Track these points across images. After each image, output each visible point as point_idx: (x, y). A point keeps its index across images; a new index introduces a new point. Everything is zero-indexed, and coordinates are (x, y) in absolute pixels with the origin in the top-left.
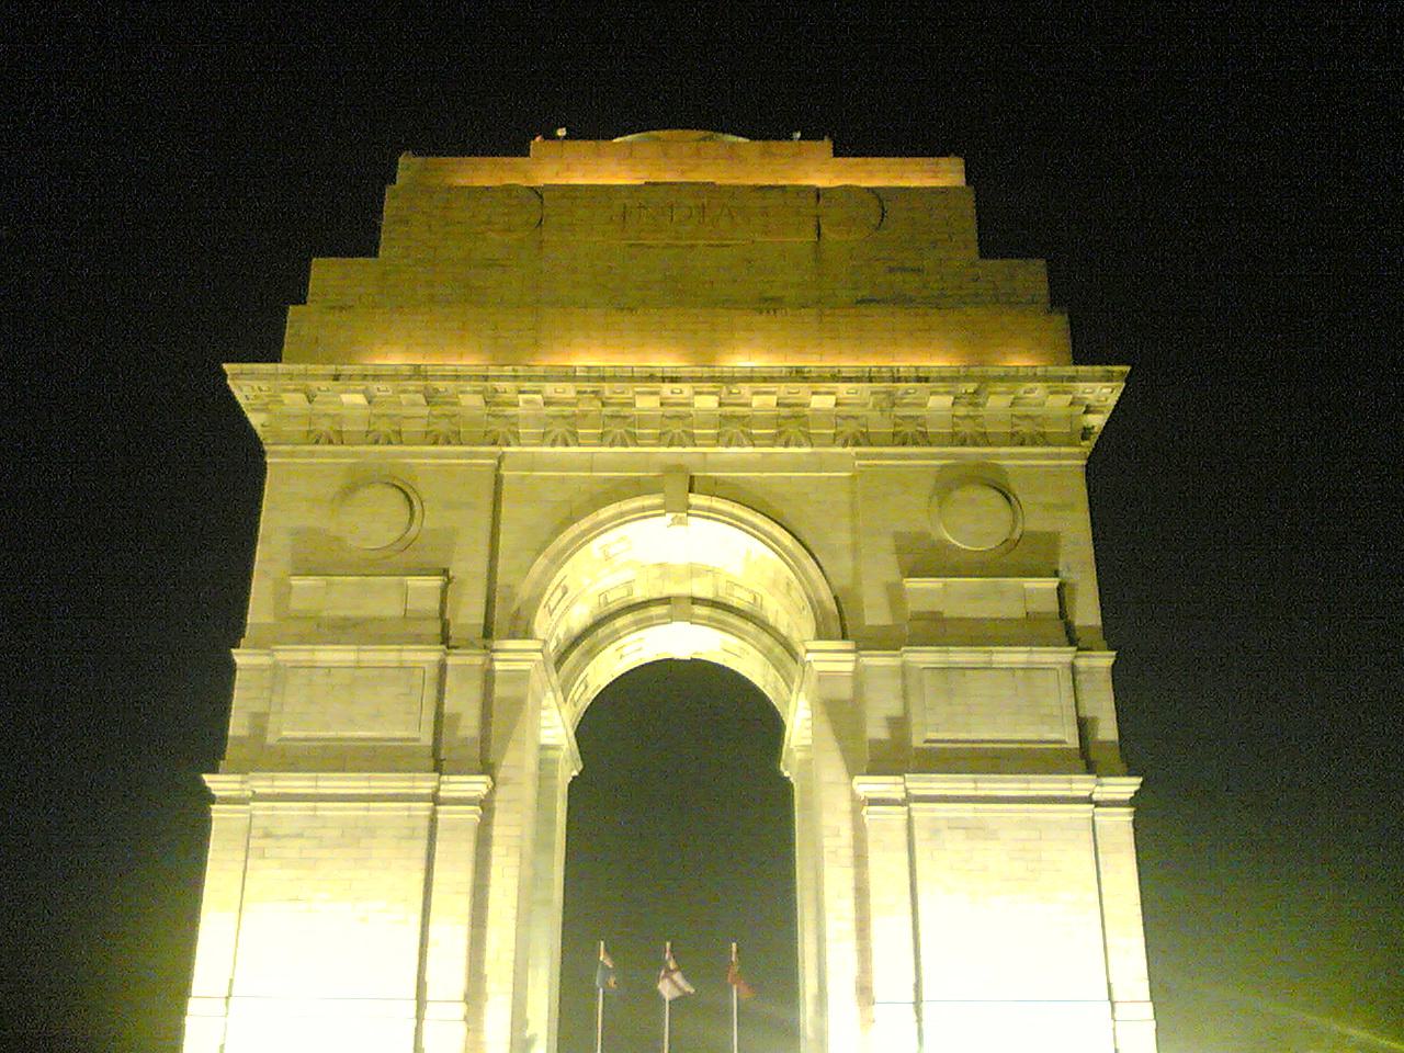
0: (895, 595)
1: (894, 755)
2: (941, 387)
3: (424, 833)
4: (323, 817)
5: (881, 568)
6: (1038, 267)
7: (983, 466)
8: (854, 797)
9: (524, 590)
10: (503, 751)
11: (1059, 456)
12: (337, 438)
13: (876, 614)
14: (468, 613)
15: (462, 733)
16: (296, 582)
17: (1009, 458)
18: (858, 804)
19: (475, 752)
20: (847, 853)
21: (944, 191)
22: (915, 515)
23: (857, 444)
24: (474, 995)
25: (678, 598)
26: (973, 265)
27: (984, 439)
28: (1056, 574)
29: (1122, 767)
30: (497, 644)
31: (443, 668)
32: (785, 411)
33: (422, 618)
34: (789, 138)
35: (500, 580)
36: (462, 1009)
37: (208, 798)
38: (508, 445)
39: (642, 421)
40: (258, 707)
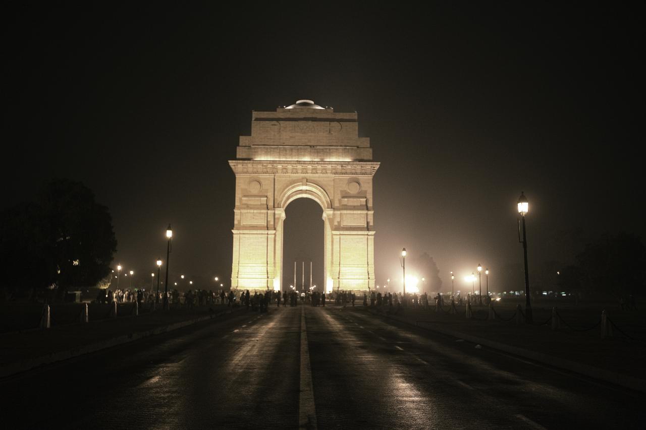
1: (338, 228)
5: (339, 196)
7: (357, 178)
8: (332, 233)
9: (279, 200)
14: (271, 204)
16: (243, 198)
17: (361, 177)
18: (333, 235)
19: (273, 226)
22: (345, 187)
24: (275, 263)
27: (356, 173)
28: (366, 197)
30: (276, 209)
33: (263, 205)
35: (276, 197)
36: (273, 265)
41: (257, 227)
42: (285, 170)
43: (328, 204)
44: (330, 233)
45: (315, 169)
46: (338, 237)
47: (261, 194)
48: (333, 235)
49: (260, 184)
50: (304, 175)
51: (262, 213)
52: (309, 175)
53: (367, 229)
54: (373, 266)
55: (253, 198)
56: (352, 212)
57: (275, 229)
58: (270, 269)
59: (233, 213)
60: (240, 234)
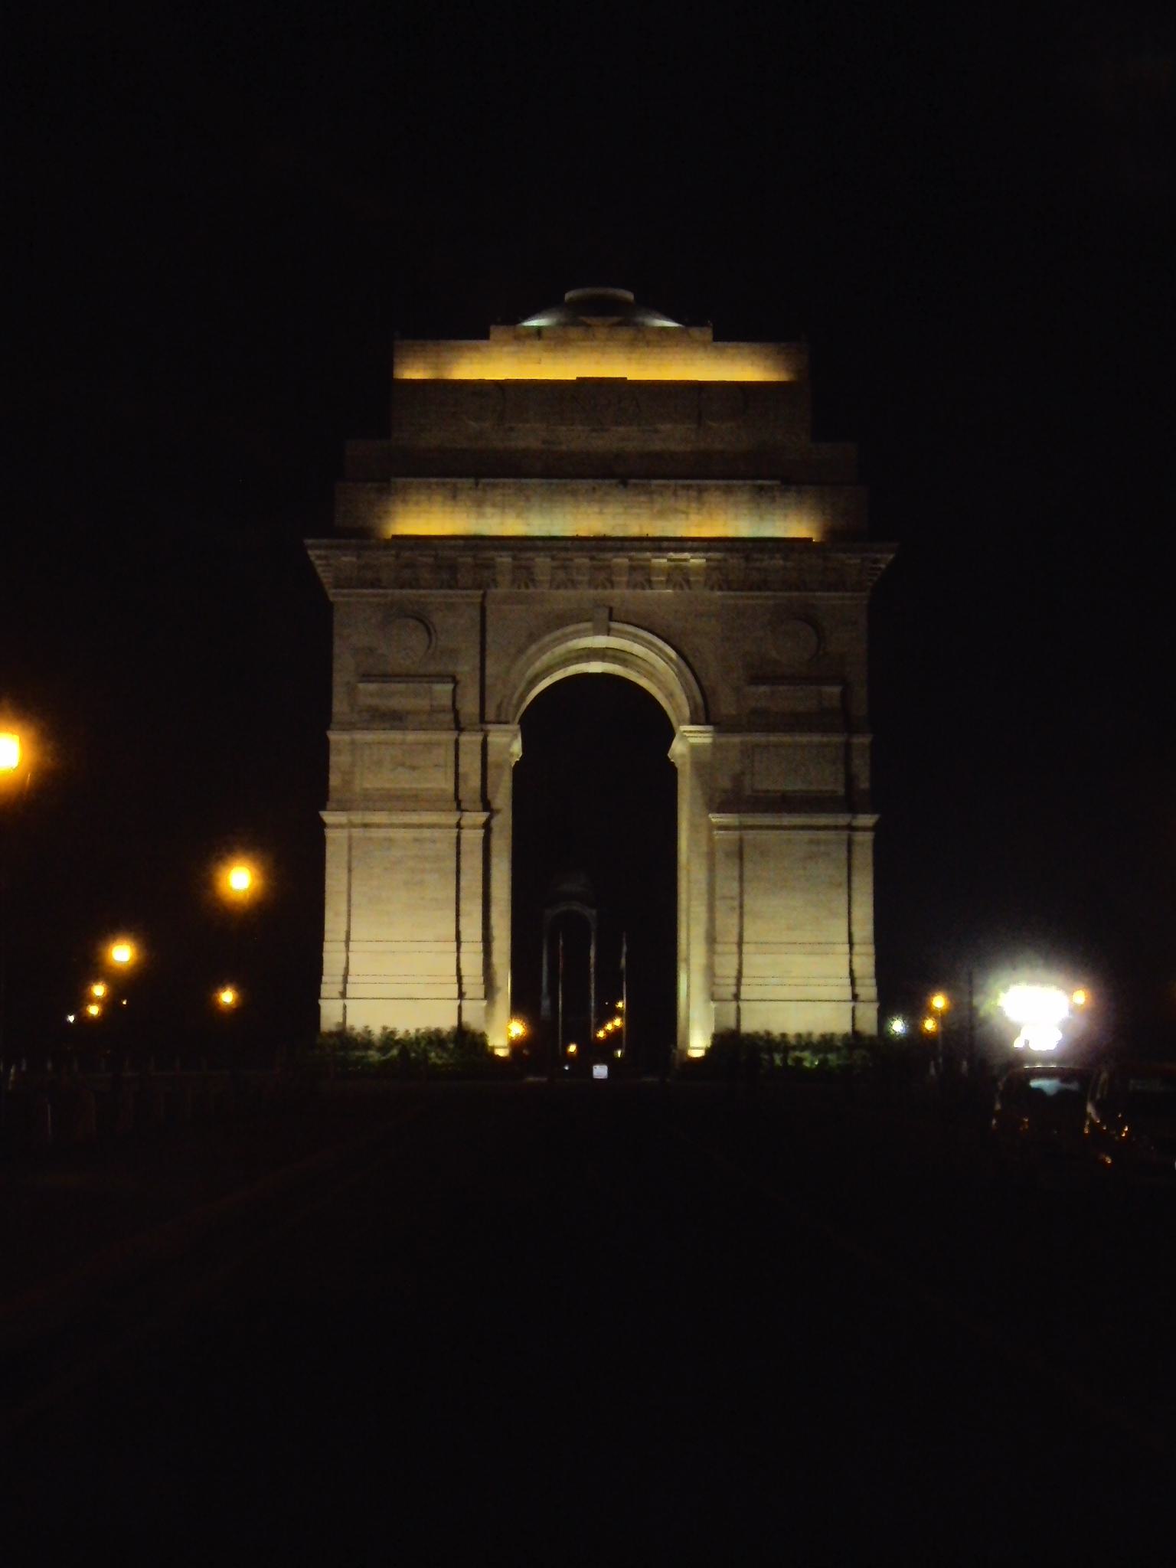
12: (375, 583)
14: (469, 706)
16: (361, 686)
19: (477, 796)
23: (721, 589)
30: (490, 727)
31: (457, 743)
32: (672, 564)
35: (489, 681)
36: (480, 947)
37: (323, 825)
38: (488, 586)
41: (416, 796)
42: (524, 575)
43: (694, 711)
46: (733, 835)
47: (433, 668)
48: (712, 827)
49: (429, 634)
50: (600, 591)
51: (438, 744)
52: (620, 594)
54: (871, 949)
55: (401, 687)
56: (787, 739)
57: (486, 805)
59: (325, 746)
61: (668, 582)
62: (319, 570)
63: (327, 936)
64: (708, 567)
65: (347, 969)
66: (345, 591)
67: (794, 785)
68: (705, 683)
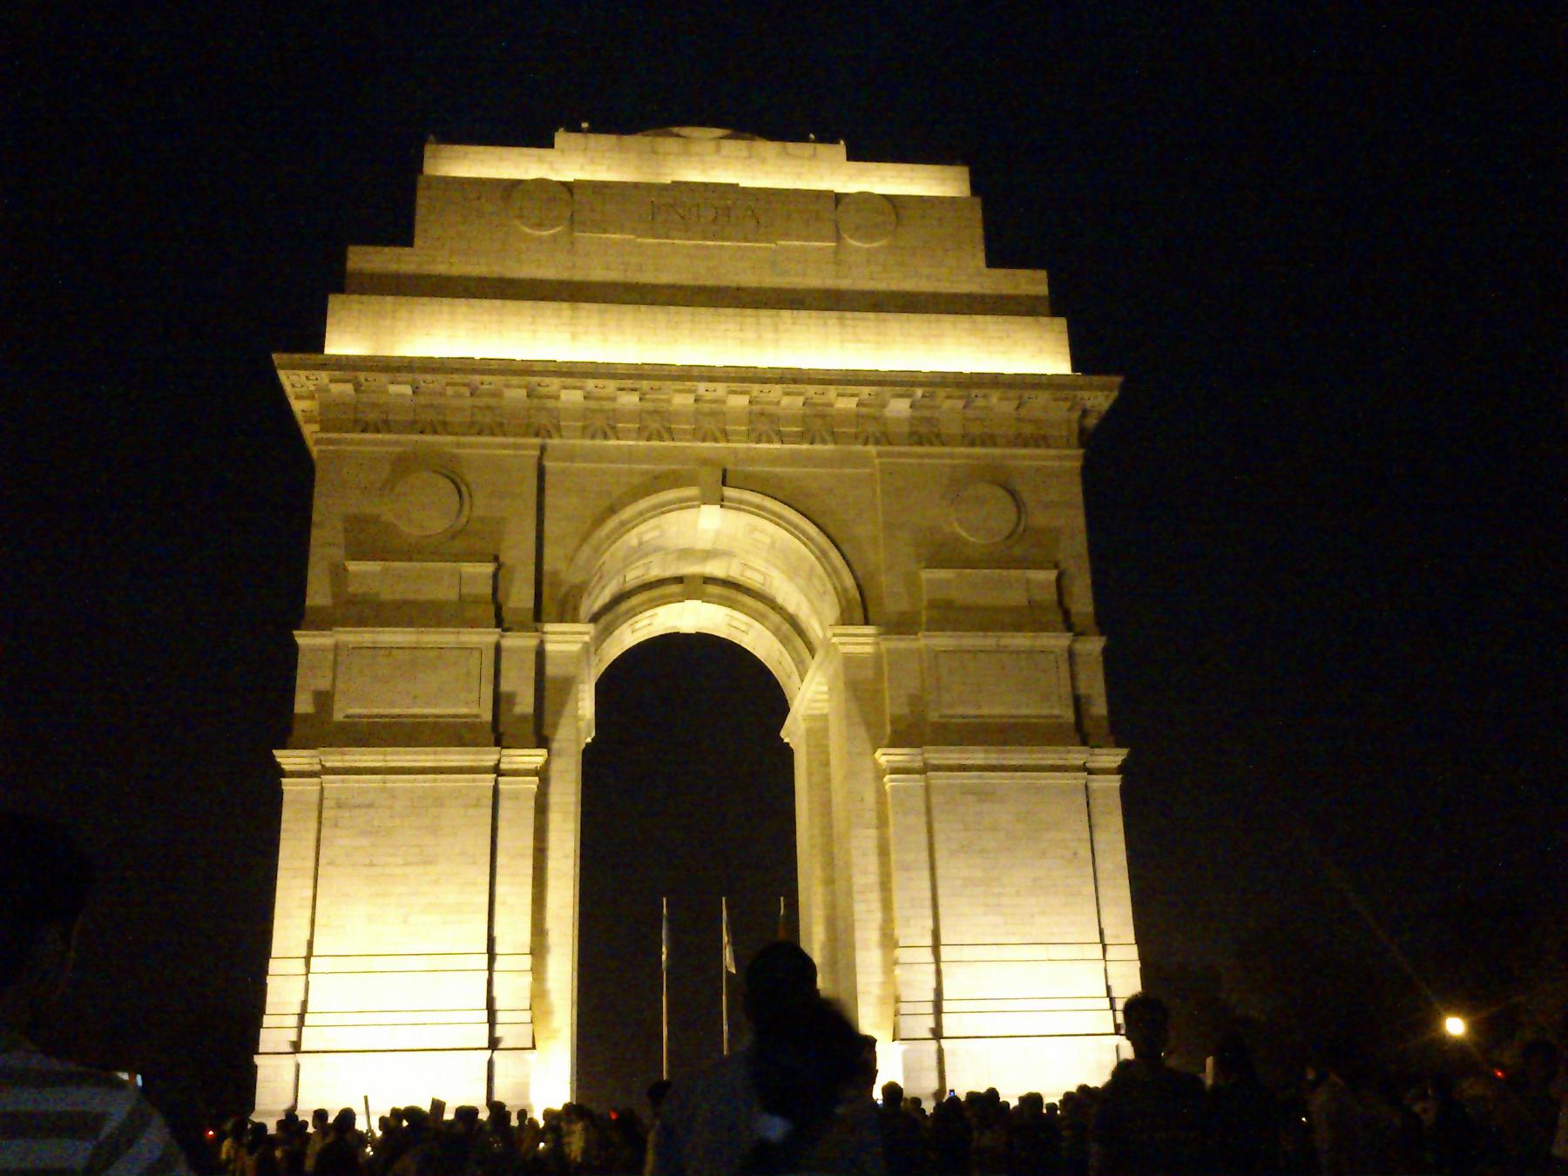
0: (912, 581)
2: (957, 392)
3: (490, 802)
4: (393, 789)
6: (1042, 275)
10: (555, 726)
11: (1060, 458)
12: (384, 426)
13: (894, 599)
14: (520, 596)
15: (518, 710)
16: (353, 566)
19: (529, 728)
20: (871, 817)
21: (952, 201)
23: (877, 443)
24: (538, 950)
25: (693, 577)
26: (979, 274)
27: (989, 440)
28: (1056, 566)
29: (1111, 739)
30: (548, 627)
31: (498, 649)
33: (477, 601)
34: (807, 140)
35: (547, 567)
36: (527, 962)
38: (550, 437)
39: (676, 415)
40: (323, 683)
44: (870, 765)
45: (773, 419)
46: (916, 781)
47: (459, 545)
48: (879, 774)
53: (1077, 738)
54: (1133, 952)
58: (513, 989)
60: (327, 771)
61: (808, 436)
62: (309, 431)
63: (276, 948)
64: (858, 415)
65: (304, 1004)
66: (334, 435)
67: (997, 708)
68: (859, 574)
